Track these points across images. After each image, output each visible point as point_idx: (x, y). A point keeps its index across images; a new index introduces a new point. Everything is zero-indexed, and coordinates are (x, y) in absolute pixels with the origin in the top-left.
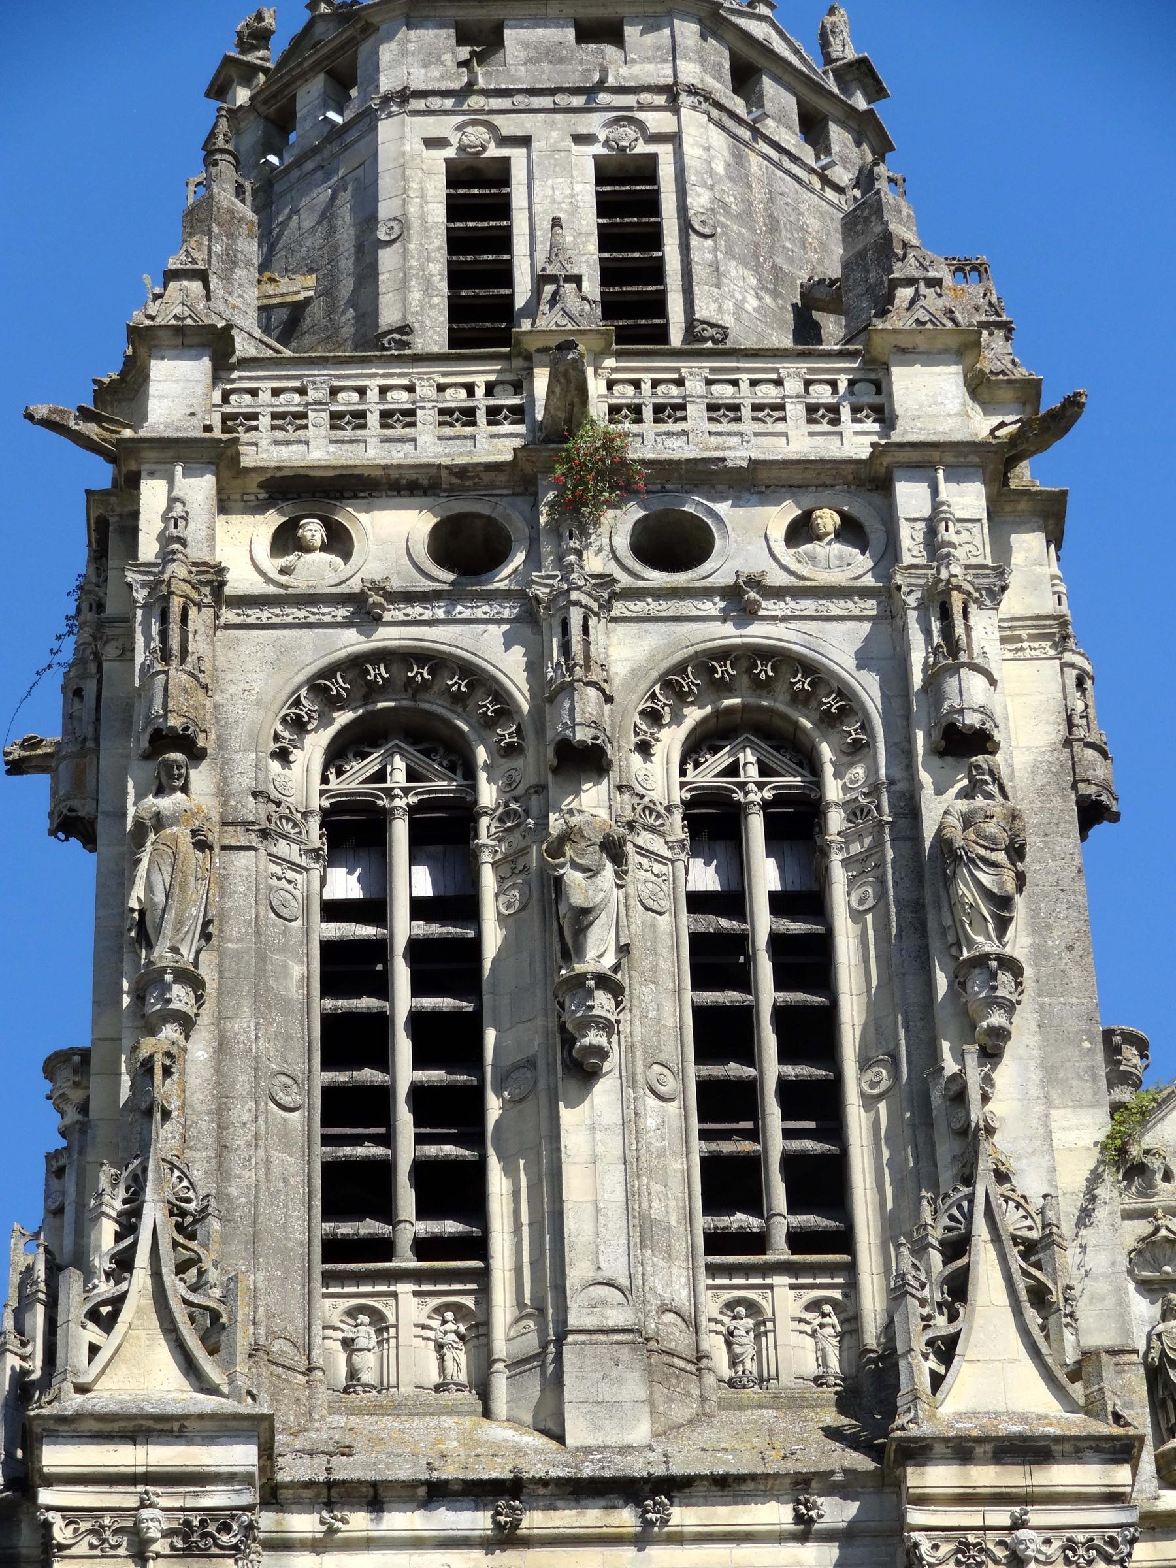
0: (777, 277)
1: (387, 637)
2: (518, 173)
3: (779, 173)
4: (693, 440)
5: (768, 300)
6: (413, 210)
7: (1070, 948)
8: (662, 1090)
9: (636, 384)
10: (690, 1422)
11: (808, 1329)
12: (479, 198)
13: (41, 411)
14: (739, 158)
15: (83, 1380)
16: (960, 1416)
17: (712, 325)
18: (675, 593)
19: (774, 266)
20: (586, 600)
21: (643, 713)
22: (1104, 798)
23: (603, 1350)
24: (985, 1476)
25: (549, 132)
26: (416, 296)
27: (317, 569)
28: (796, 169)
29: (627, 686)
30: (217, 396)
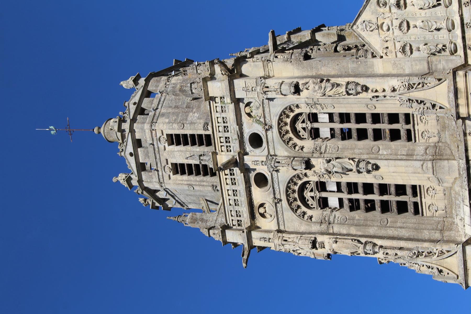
0: (189, 107)
1: (284, 198)
2: (174, 161)
3: (164, 104)
4: (233, 134)
5: (194, 110)
6: (186, 183)
7: (338, 65)
8: (377, 150)
9: (221, 146)
10: (450, 149)
11: (427, 122)
12: (179, 169)
13: (244, 265)
14: (163, 115)
15: (456, 277)
16: (449, 103)
17: (204, 126)
18: (268, 142)
19: (186, 108)
20: (273, 163)
21: (295, 149)
22: (303, 55)
23: (437, 169)
24: (462, 101)
25: (164, 155)
26: (205, 183)
27: (270, 209)
28: (162, 100)
29: (290, 152)
30: (234, 227)
